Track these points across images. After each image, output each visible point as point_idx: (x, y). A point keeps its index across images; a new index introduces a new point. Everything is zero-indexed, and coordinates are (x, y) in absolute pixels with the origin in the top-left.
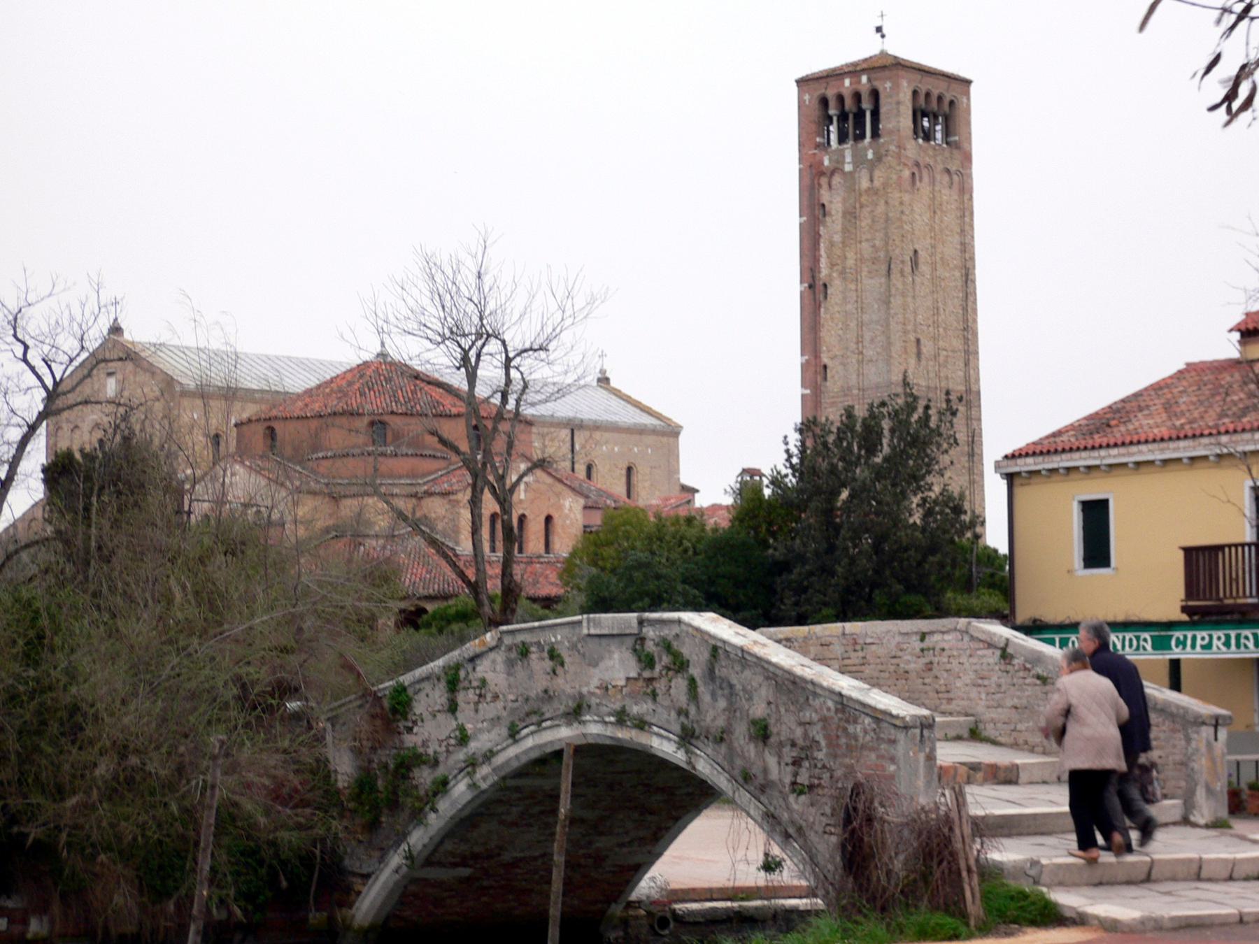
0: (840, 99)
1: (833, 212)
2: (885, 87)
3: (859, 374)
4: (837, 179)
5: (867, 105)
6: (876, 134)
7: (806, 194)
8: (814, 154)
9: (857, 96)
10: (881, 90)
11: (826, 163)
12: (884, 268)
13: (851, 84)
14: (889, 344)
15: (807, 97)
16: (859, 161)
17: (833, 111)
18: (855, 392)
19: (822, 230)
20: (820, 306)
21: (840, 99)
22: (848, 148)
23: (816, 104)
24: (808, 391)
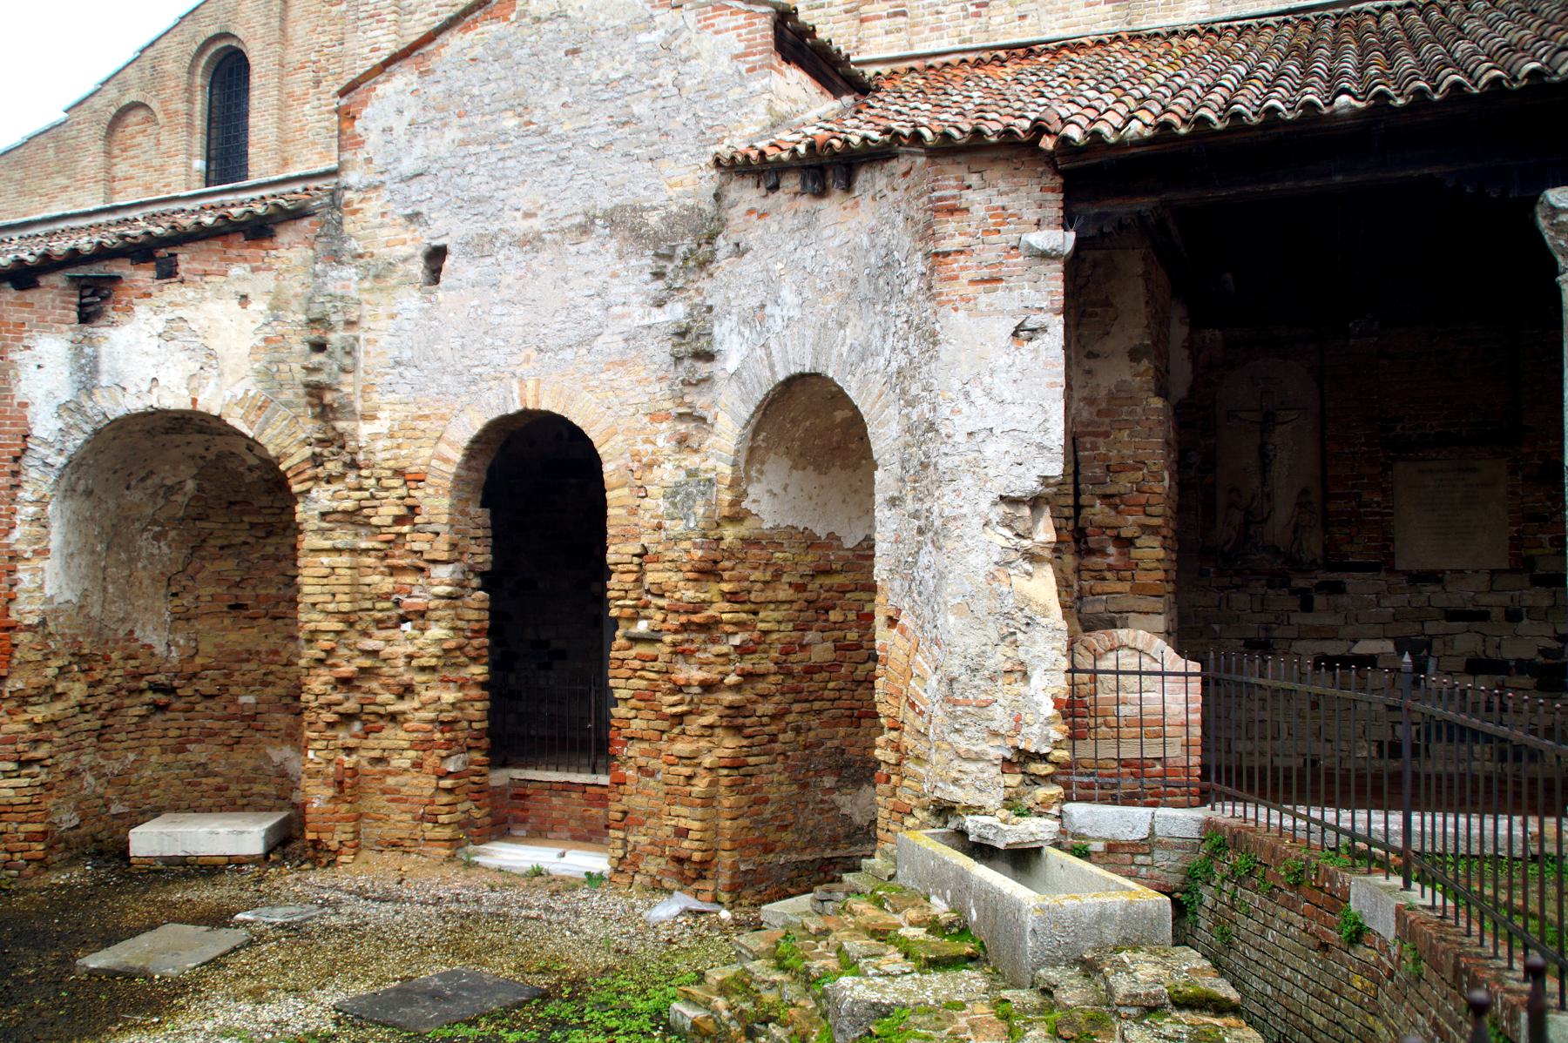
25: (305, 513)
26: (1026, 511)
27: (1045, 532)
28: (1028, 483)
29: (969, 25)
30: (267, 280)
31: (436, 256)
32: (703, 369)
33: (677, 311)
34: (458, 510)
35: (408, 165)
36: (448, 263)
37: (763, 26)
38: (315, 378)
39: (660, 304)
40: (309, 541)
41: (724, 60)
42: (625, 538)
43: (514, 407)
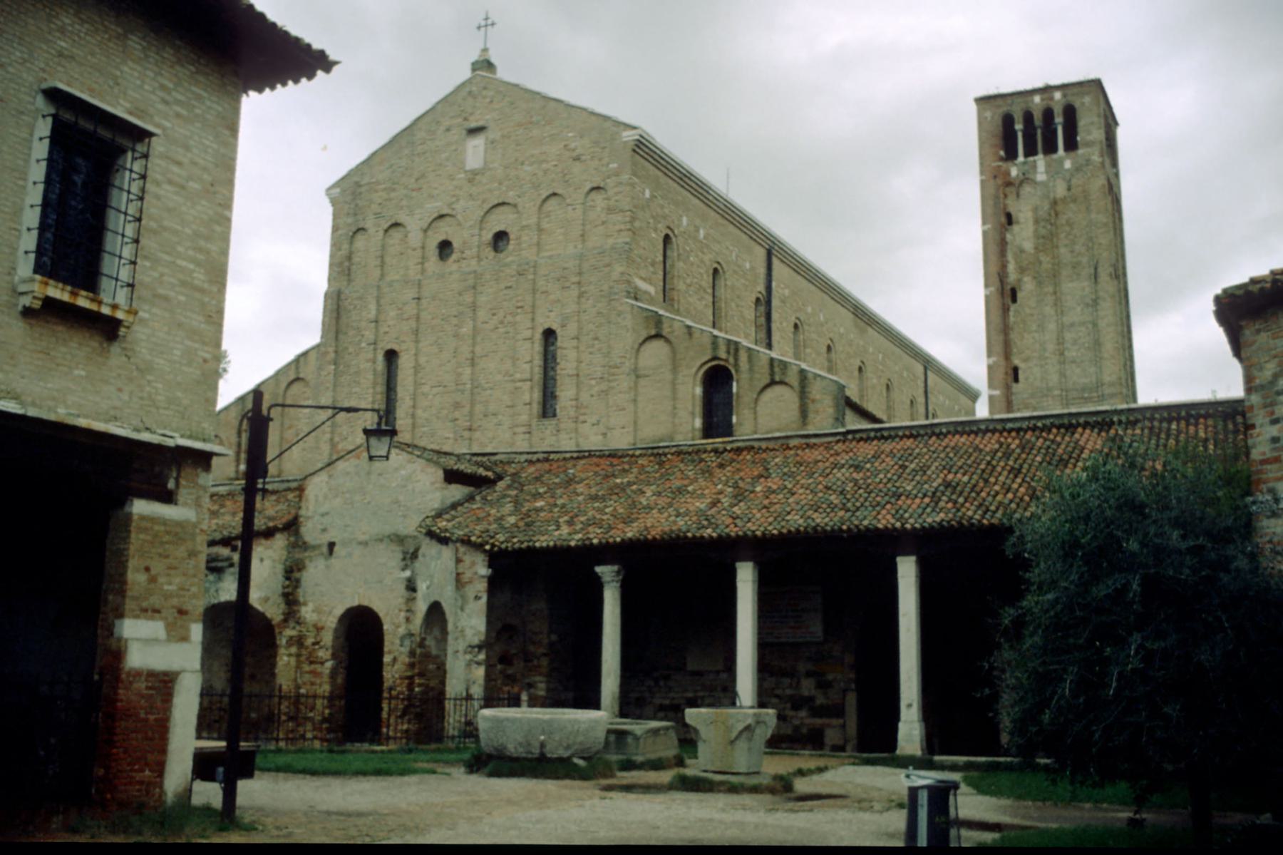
0: (1028, 117)
1: (1022, 220)
2: (1084, 104)
3: (1063, 375)
4: (1027, 189)
5: (1059, 120)
6: (1071, 145)
7: (991, 203)
8: (999, 167)
9: (1048, 114)
10: (1077, 105)
11: (1014, 172)
12: (1087, 271)
13: (1042, 100)
14: (1097, 344)
15: (988, 114)
16: (1053, 171)
17: (1019, 127)
18: (1057, 392)
19: (1009, 237)
20: (1008, 309)
21: (1028, 117)
22: (1040, 160)
23: (998, 121)
24: (997, 393)
25: (282, 641)
26: (476, 650)
27: (482, 657)
28: (476, 641)
29: (554, 438)
30: (270, 552)
31: (331, 546)
32: (414, 595)
33: (408, 573)
34: (336, 638)
35: (323, 510)
36: (336, 549)
37: (441, 474)
38: (286, 590)
39: (403, 570)
40: (282, 651)
41: (428, 484)
42: (390, 652)
43: (356, 603)
